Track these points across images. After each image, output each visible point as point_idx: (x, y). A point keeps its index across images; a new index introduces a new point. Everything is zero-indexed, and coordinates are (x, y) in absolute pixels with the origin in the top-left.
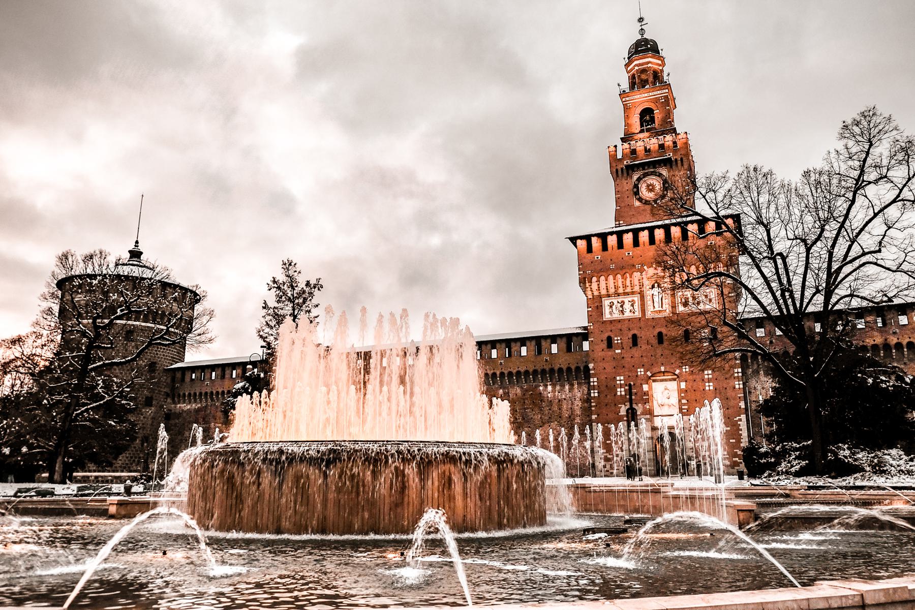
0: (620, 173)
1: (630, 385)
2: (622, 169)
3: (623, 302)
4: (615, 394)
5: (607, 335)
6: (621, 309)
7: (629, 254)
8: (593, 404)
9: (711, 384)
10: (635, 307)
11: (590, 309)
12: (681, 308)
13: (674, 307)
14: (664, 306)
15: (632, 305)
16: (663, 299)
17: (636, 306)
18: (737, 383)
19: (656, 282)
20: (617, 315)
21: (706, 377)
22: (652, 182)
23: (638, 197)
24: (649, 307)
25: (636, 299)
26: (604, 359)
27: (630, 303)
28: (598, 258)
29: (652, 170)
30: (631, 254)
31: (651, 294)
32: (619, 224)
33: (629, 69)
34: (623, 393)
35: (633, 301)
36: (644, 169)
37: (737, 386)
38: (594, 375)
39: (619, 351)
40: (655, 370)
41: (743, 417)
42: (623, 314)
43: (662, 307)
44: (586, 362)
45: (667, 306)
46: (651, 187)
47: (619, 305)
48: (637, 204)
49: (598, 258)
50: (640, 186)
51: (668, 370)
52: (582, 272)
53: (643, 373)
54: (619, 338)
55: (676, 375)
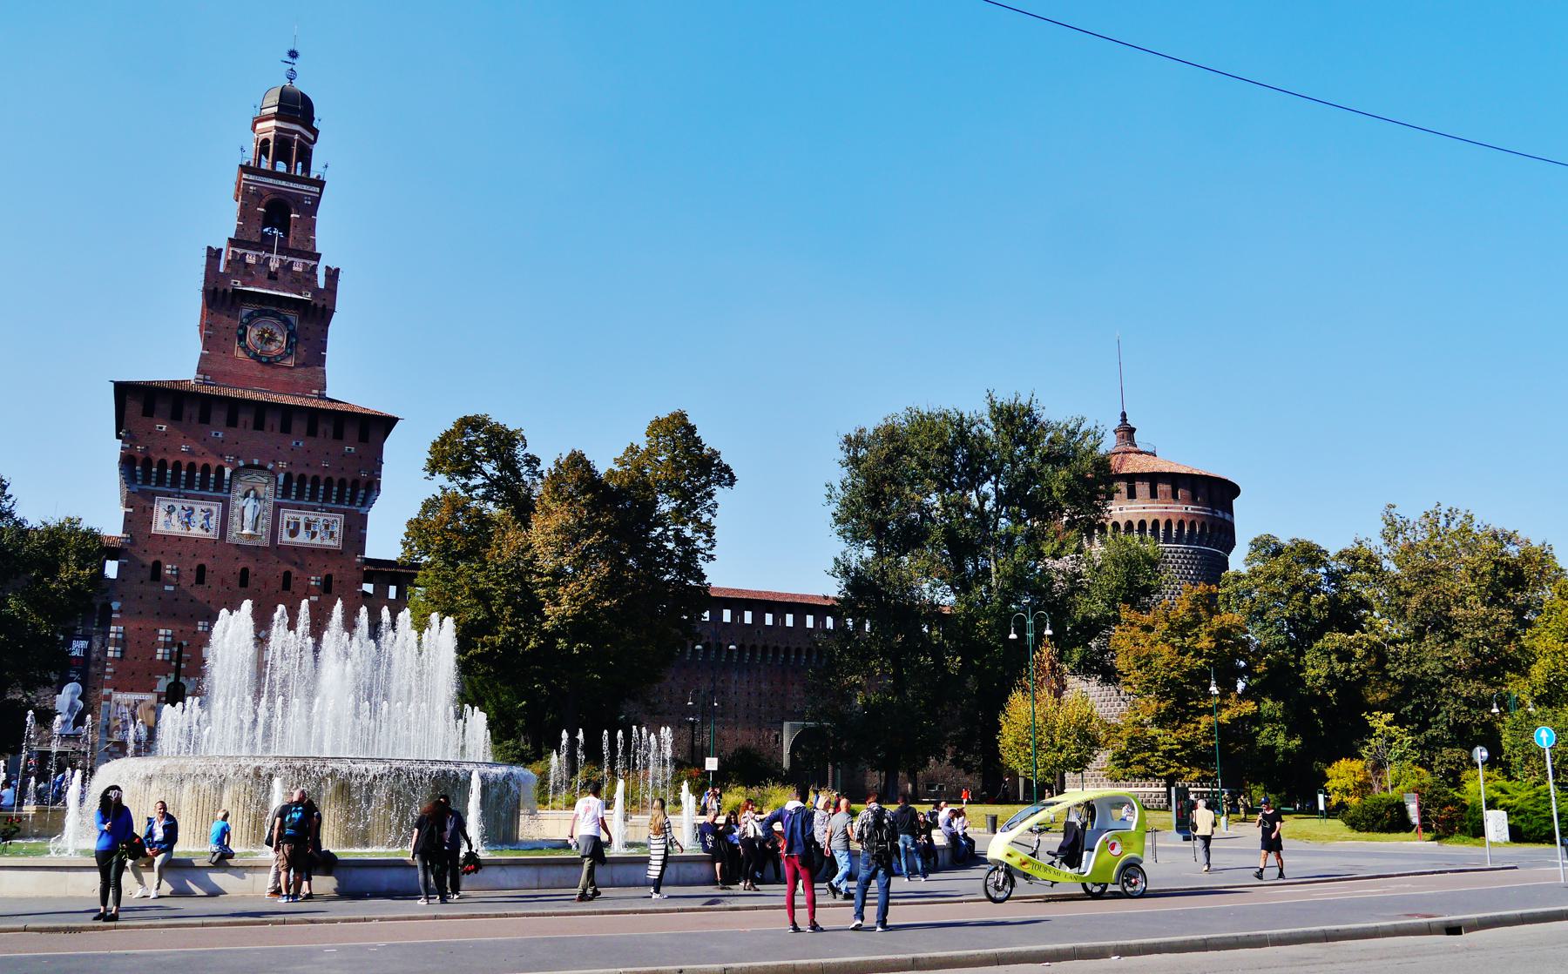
1: (180, 646)
3: (192, 509)
4: (153, 658)
5: (153, 559)
6: (186, 520)
7: (217, 434)
8: (108, 670)
11: (131, 510)
12: (285, 538)
14: (259, 529)
15: (207, 518)
16: (261, 516)
17: (213, 521)
19: (253, 489)
20: (177, 529)
24: (234, 526)
25: (214, 509)
26: (141, 597)
27: (204, 514)
28: (161, 428)
29: (274, 309)
30: (220, 435)
31: (241, 506)
33: (259, 126)
34: (167, 657)
35: (209, 510)
38: (118, 622)
39: (172, 588)
42: (189, 530)
43: (255, 529)
45: (264, 530)
47: (184, 513)
48: (240, 354)
49: (161, 428)
50: (249, 327)
52: (128, 446)
54: (175, 567)
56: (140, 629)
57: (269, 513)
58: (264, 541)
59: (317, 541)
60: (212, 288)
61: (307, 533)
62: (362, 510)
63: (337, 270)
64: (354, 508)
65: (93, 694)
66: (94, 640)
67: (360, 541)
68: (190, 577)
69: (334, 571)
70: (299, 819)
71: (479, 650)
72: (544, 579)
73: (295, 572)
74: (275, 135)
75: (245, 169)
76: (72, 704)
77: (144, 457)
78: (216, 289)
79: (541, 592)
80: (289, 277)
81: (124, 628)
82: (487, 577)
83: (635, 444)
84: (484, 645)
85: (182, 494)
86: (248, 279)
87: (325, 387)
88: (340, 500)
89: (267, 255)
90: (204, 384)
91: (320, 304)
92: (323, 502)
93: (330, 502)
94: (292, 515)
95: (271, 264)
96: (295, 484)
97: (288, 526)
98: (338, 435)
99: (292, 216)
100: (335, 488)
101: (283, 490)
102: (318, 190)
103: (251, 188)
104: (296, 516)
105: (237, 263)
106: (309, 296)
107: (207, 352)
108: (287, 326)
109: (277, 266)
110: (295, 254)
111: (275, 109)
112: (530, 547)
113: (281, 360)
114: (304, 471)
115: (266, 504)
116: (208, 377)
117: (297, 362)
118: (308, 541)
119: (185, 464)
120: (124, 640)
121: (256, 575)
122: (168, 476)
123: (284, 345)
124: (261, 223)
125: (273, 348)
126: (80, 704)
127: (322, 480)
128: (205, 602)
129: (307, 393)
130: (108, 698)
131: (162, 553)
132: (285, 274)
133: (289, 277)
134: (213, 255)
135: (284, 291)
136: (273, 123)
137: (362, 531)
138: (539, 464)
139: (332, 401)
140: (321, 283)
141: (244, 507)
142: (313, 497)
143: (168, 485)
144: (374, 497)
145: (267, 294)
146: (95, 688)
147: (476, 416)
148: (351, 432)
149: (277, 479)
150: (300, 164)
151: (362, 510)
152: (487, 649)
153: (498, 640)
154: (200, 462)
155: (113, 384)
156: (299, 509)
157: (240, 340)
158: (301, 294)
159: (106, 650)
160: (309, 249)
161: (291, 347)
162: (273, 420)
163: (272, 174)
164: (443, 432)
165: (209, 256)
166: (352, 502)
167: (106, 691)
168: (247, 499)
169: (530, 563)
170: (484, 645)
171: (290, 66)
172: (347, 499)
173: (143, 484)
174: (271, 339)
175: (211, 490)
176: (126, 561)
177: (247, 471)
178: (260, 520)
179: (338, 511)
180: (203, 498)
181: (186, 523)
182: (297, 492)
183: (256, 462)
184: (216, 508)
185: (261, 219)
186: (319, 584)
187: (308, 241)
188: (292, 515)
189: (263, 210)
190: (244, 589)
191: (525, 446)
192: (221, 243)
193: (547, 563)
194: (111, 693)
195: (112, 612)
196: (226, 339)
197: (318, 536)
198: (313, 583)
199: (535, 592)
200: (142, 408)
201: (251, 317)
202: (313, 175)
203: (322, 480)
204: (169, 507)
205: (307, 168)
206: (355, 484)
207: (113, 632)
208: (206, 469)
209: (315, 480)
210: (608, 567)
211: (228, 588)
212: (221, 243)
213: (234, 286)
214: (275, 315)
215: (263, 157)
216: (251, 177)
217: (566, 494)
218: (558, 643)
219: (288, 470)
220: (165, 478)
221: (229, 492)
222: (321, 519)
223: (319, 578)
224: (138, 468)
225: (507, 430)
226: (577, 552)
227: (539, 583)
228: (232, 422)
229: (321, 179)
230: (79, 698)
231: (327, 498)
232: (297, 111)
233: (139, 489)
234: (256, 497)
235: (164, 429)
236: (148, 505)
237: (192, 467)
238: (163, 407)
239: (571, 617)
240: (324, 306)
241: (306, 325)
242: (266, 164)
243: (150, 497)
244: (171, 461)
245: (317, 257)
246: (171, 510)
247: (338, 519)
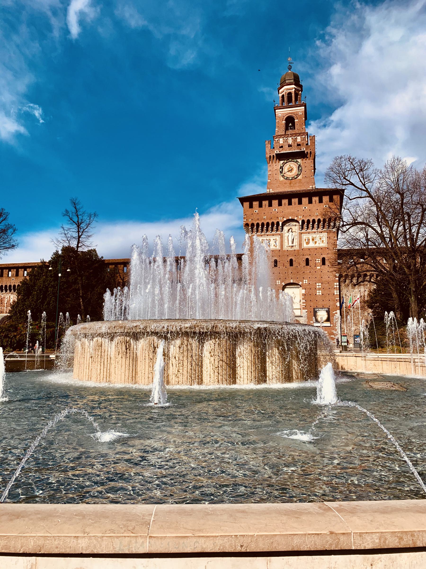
0: (272, 158)
2: (273, 156)
3: (270, 240)
9: (320, 291)
12: (305, 245)
13: (300, 245)
18: (335, 291)
21: (318, 287)
23: (282, 174)
33: (280, 91)
37: (336, 293)
41: (338, 311)
45: (296, 243)
46: (290, 169)
48: (282, 179)
53: (279, 283)
59: (317, 245)
86: (281, 149)
102: (303, 108)
109: (291, 142)
133: (296, 144)
149: (299, 223)
154: (270, 222)
157: (281, 173)
183: (290, 218)
184: (278, 238)
188: (306, 236)
197: (317, 243)
198: (317, 262)
208: (273, 224)
219: (303, 219)
240: (311, 152)
241: (305, 161)
247: (325, 235)
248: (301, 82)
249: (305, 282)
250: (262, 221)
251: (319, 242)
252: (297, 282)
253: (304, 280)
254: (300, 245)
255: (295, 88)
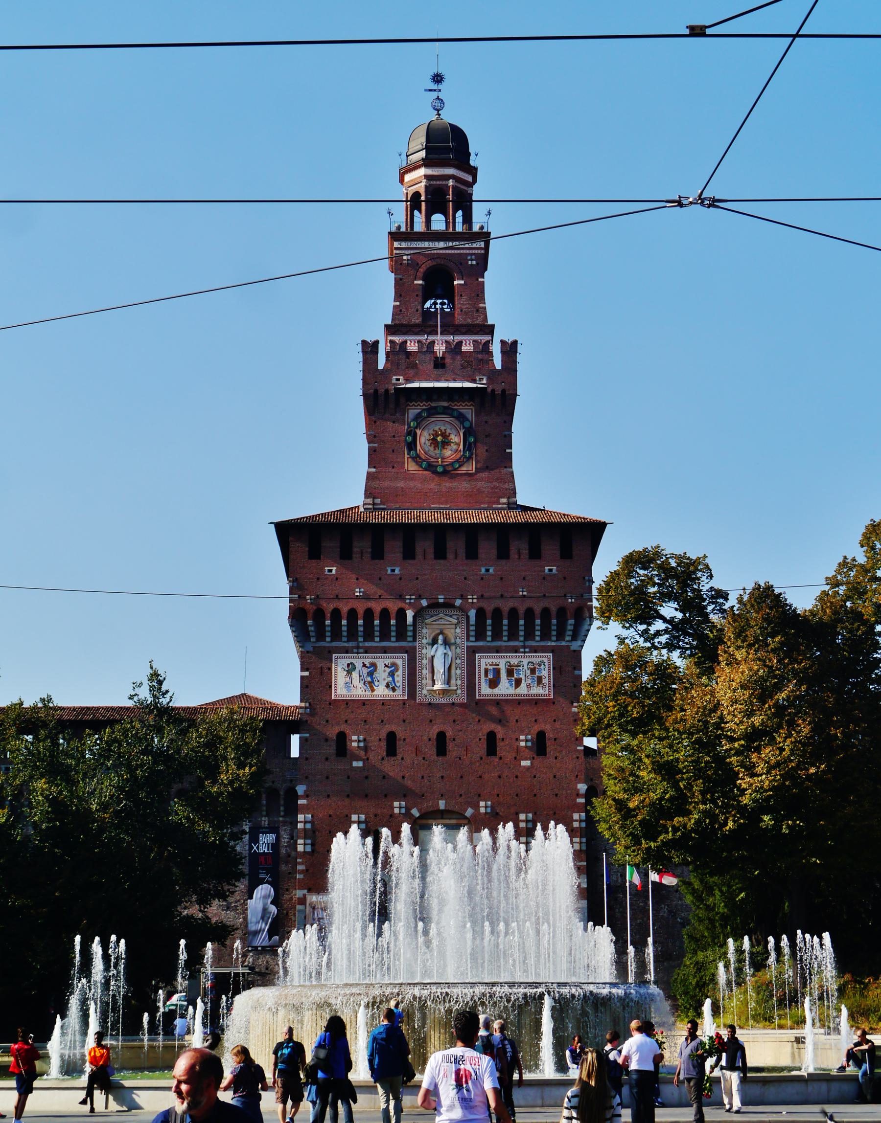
3: (374, 665)
6: (369, 679)
7: (393, 571)
8: (299, 867)
10: (396, 679)
11: (307, 674)
12: (485, 690)
13: (471, 686)
14: (453, 682)
15: (392, 674)
17: (399, 677)
19: (442, 633)
20: (359, 691)
22: (443, 428)
24: (424, 682)
25: (399, 662)
27: (388, 670)
28: (330, 571)
29: (445, 404)
30: (397, 571)
31: (429, 656)
32: (374, 504)
33: (408, 178)
35: (394, 664)
36: (429, 399)
38: (305, 809)
39: (360, 764)
40: (427, 805)
42: (373, 690)
44: (291, 781)
45: (459, 682)
47: (365, 671)
48: (411, 467)
50: (418, 432)
51: (451, 808)
54: (361, 738)
55: (466, 818)
56: (330, 816)
57: (462, 662)
58: (461, 696)
59: (523, 690)
60: (372, 391)
61: (510, 681)
62: (574, 646)
63: (515, 343)
64: (563, 643)
65: (286, 897)
66: (282, 833)
67: (575, 686)
68: (379, 748)
69: (547, 727)
70: (289, 1054)
71: (670, 834)
72: (736, 745)
73: (500, 732)
74: (426, 187)
75: (395, 236)
76: (265, 910)
77: (315, 608)
78: (376, 391)
79: (734, 759)
80: (459, 361)
81: (312, 816)
82: (671, 746)
83: (850, 557)
84: (675, 829)
85: (361, 648)
86: (412, 372)
87: (515, 493)
88: (545, 636)
89: (431, 338)
90: (374, 509)
91: (499, 391)
92: (526, 639)
93: (534, 639)
94: (490, 661)
95: (437, 348)
96: (489, 622)
97: (486, 675)
98: (535, 554)
99: (456, 283)
100: (538, 622)
101: (476, 631)
103: (405, 257)
104: (495, 661)
105: (397, 353)
106: (484, 382)
107: (373, 470)
108: (462, 423)
109: (443, 348)
110: (464, 331)
111: (423, 154)
112: (717, 705)
113: (460, 466)
114: (499, 603)
115: (458, 651)
116: (378, 501)
117: (478, 467)
118: (511, 691)
119: (361, 611)
120: (314, 830)
121: (454, 740)
122: (344, 629)
123: (461, 447)
124: (420, 299)
125: (448, 453)
126: (273, 909)
127: (521, 612)
128: (399, 778)
129: (494, 503)
130: (302, 901)
131: (346, 721)
132: (453, 359)
133: (459, 361)
134: (370, 349)
135: (455, 380)
136: (422, 171)
137: (576, 672)
138: (726, 599)
139: (525, 509)
140: (498, 363)
141: (433, 657)
142: (513, 636)
143: (344, 639)
144: (586, 627)
145: (434, 388)
146: (287, 890)
147: (645, 550)
148: (550, 548)
149: (468, 618)
150: (459, 214)
151: (574, 646)
152: (679, 833)
153: (691, 824)
154: (377, 607)
155: (273, 526)
156: (497, 652)
157: (410, 450)
158: (474, 381)
159: (296, 844)
160: (479, 321)
161: (469, 449)
162: (456, 545)
163: (430, 235)
164: (608, 574)
165: (364, 352)
166: (560, 636)
167: (299, 893)
168: (435, 646)
169: (718, 726)
170: (675, 829)
171: (435, 95)
172: (554, 633)
173: (318, 640)
174: (446, 443)
175: (393, 639)
176: (307, 735)
177: (433, 611)
178: (453, 671)
179: (544, 650)
180: (385, 650)
181: (369, 683)
182: (492, 631)
184: (401, 661)
185: (420, 293)
186: (529, 744)
187: (478, 311)
188: (490, 661)
189: (420, 282)
190: (441, 758)
191: (711, 576)
192: (377, 334)
193: (736, 724)
194: (305, 895)
195: (297, 797)
196: (393, 451)
197: (523, 684)
198: (523, 744)
199: (728, 760)
200: (307, 549)
201: (419, 419)
202: (476, 228)
203: (521, 612)
204: (348, 665)
205: (468, 219)
206: (562, 613)
207: (301, 822)
208: (385, 614)
209: (513, 614)
210: (809, 724)
211: (424, 758)
212: (377, 334)
213: (396, 384)
214: (446, 411)
215: (416, 213)
216: (404, 245)
217: (751, 639)
218: (762, 820)
219: (479, 605)
220: (341, 631)
221: (414, 640)
222: (525, 662)
223: (529, 737)
224: (310, 622)
225: (689, 558)
226: (770, 708)
227: (731, 749)
228: (409, 554)
229: (485, 230)
230: (272, 903)
231: (529, 635)
232: (447, 150)
233: (314, 647)
234: (446, 643)
235: (334, 572)
236: (323, 664)
237: (369, 614)
238: (331, 545)
239: (770, 790)
240: (504, 391)
242: (419, 226)
243: (326, 655)
244: (345, 610)
245: (490, 330)
246: (350, 669)
247: (546, 660)
248: (472, 157)
249: (482, 810)
250: (353, 604)
251: (529, 681)
252: (456, 808)
253: (482, 804)
254: (471, 686)
255: (452, 177)
